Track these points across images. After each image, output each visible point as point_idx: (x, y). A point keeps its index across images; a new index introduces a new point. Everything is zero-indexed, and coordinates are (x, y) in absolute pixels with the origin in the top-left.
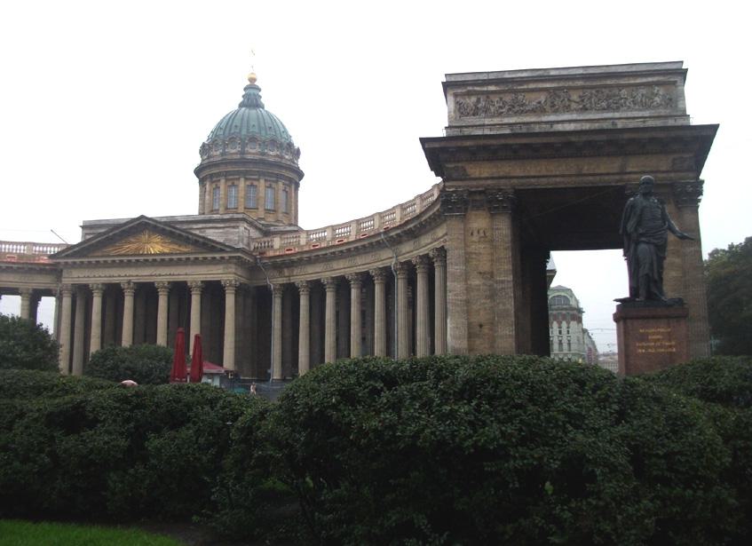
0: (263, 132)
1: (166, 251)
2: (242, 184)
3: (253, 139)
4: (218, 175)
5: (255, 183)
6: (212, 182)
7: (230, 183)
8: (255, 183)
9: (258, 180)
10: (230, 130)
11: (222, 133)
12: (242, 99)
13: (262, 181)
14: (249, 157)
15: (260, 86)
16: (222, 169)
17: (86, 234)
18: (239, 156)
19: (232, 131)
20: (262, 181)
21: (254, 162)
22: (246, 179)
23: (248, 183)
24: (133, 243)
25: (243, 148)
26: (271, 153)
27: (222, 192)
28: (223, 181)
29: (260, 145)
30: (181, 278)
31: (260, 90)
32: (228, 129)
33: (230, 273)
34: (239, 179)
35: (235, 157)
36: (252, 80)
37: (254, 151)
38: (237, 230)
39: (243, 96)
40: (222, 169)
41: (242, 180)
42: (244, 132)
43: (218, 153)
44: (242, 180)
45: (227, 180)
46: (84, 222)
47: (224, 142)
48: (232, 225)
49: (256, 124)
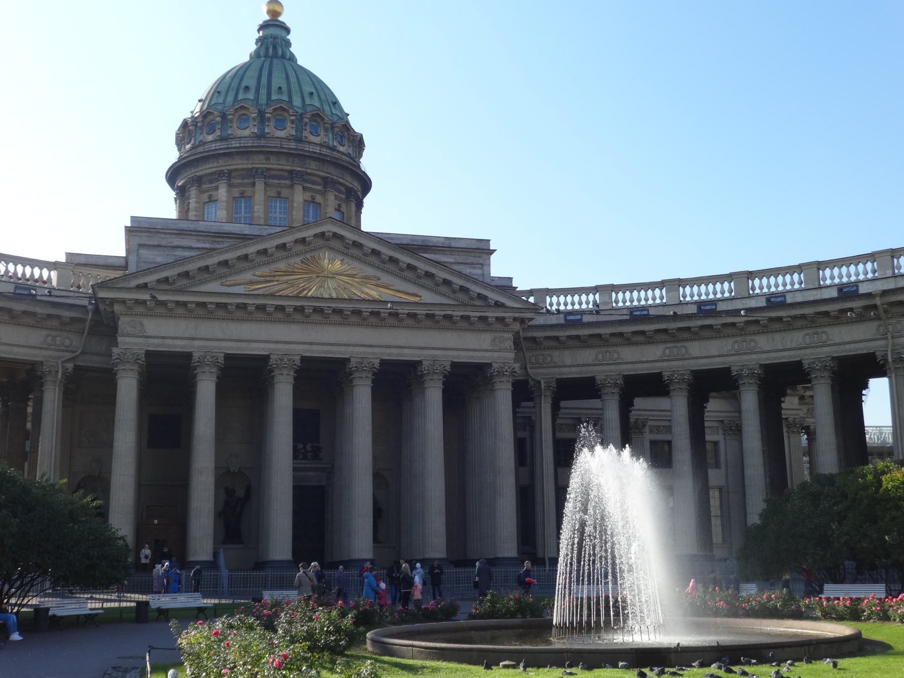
0: (326, 108)
1: (374, 293)
2: (299, 196)
3: (317, 117)
4: (253, 173)
5: (319, 199)
6: (230, 186)
7: (273, 193)
8: (319, 199)
9: (323, 193)
10: (269, 95)
11: (251, 95)
12: (253, 47)
13: (331, 196)
14: (307, 148)
15: (288, 24)
16: (259, 162)
17: (141, 246)
18: (293, 145)
19: (274, 97)
20: (331, 196)
21: (321, 159)
22: (304, 189)
23: (308, 196)
24: (293, 273)
25: (299, 130)
26: (341, 149)
27: (259, 209)
28: (260, 186)
29: (326, 130)
30: (408, 355)
31: (288, 31)
32: (263, 92)
33: (500, 350)
34: (291, 187)
35: (286, 145)
36: (274, 14)
37: (316, 140)
38: (479, 272)
39: (258, 41)
40: (259, 162)
41: (298, 189)
42: (297, 102)
43: (247, 133)
44: (298, 189)
45: (265, 183)
46: (134, 219)
47: (261, 114)
48: (471, 260)
49: (313, 90)
